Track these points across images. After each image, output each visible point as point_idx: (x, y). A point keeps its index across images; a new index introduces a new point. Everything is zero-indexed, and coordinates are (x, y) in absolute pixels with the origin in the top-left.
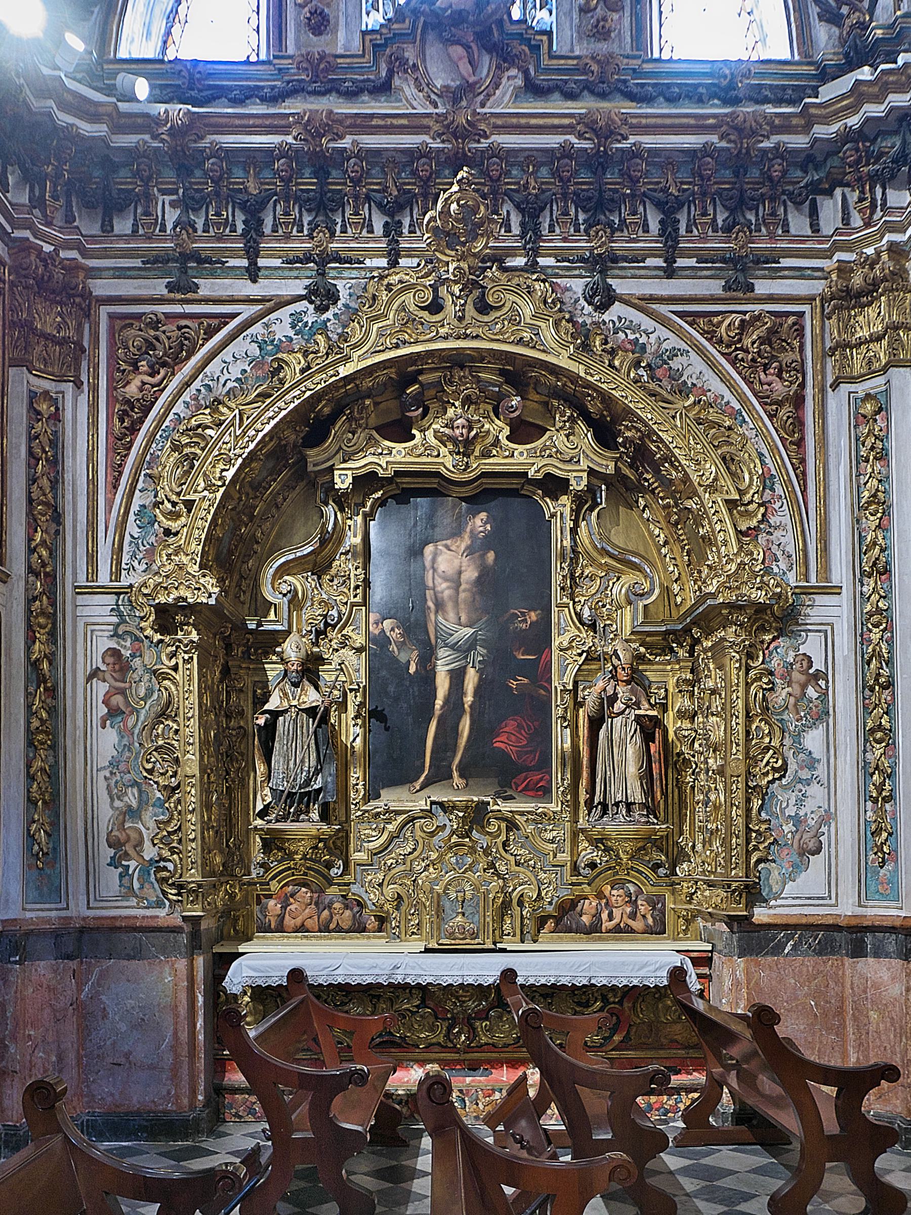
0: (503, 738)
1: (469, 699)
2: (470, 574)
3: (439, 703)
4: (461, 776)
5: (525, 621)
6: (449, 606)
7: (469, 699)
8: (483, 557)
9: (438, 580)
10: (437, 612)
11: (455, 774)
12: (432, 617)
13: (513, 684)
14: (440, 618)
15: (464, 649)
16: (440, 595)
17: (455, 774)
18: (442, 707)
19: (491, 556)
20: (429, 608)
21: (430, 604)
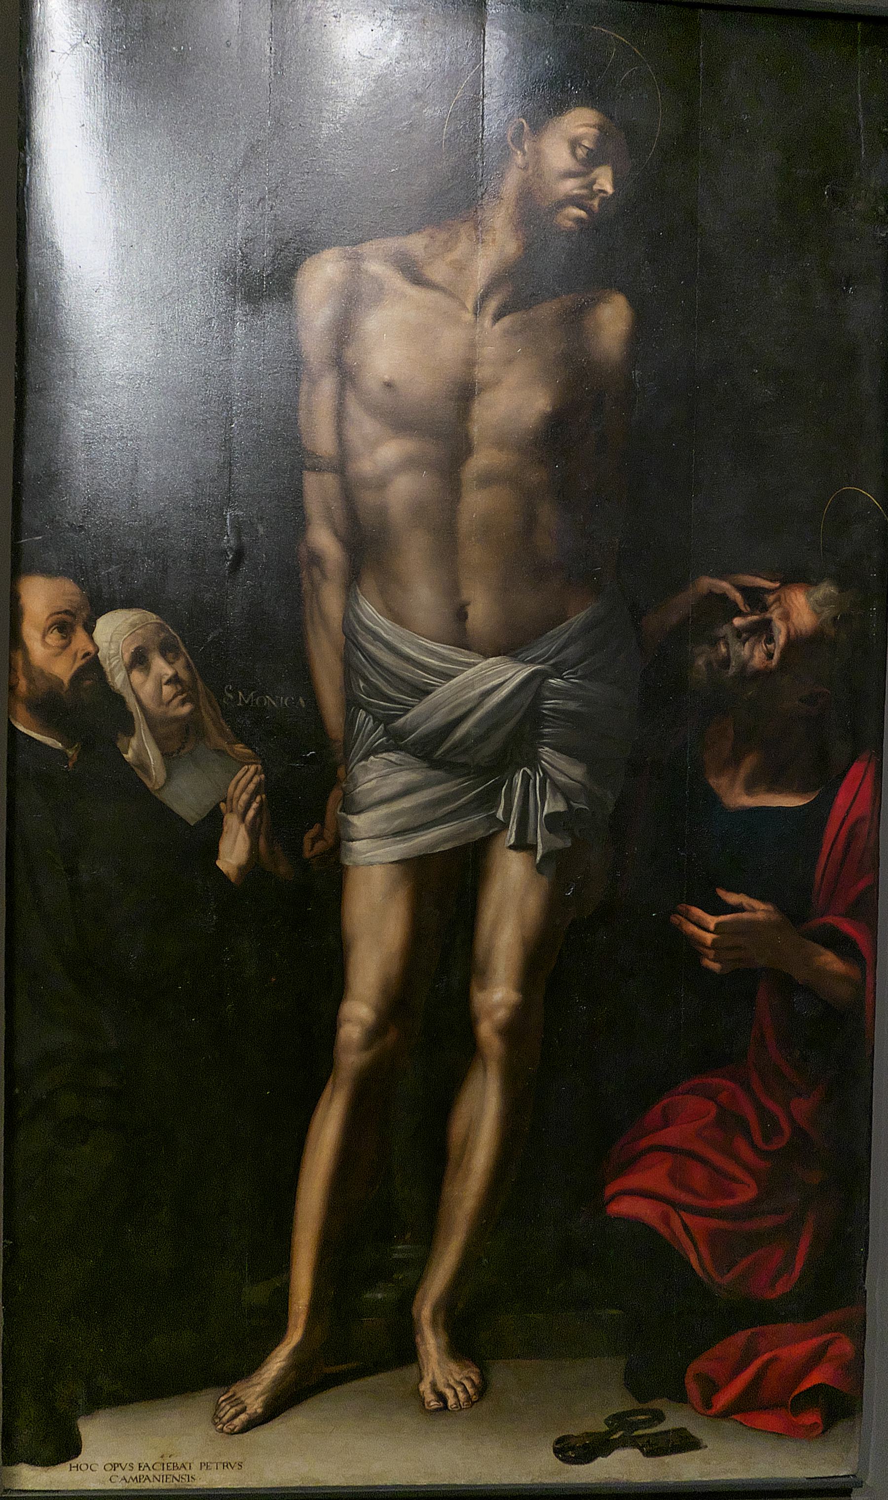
0: (653, 1176)
1: (498, 996)
2: (516, 400)
3: (358, 1012)
4: (462, 1346)
5: (762, 630)
6: (415, 556)
7: (498, 996)
8: (575, 320)
9: (364, 426)
10: (353, 578)
11: (431, 1344)
12: (331, 600)
13: (704, 926)
14: (370, 611)
15: (477, 761)
16: (368, 498)
17: (431, 1344)
18: (375, 1033)
19: (613, 319)
20: (316, 559)
21: (324, 540)
